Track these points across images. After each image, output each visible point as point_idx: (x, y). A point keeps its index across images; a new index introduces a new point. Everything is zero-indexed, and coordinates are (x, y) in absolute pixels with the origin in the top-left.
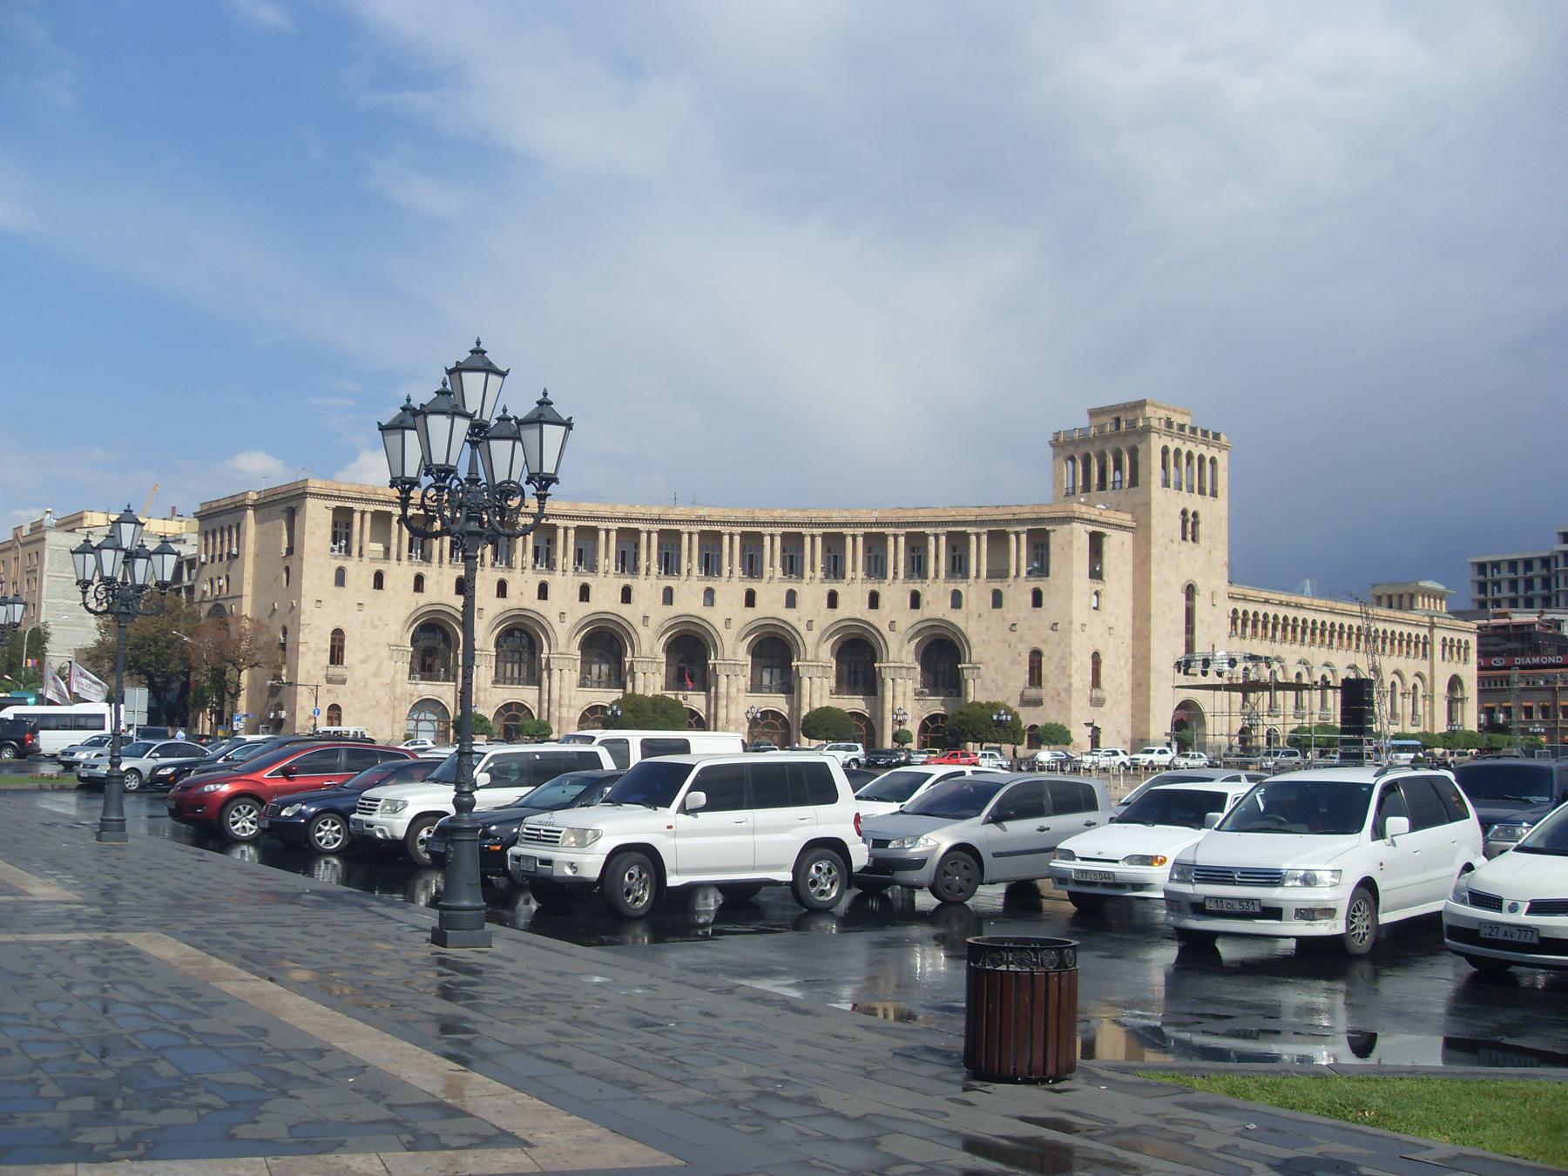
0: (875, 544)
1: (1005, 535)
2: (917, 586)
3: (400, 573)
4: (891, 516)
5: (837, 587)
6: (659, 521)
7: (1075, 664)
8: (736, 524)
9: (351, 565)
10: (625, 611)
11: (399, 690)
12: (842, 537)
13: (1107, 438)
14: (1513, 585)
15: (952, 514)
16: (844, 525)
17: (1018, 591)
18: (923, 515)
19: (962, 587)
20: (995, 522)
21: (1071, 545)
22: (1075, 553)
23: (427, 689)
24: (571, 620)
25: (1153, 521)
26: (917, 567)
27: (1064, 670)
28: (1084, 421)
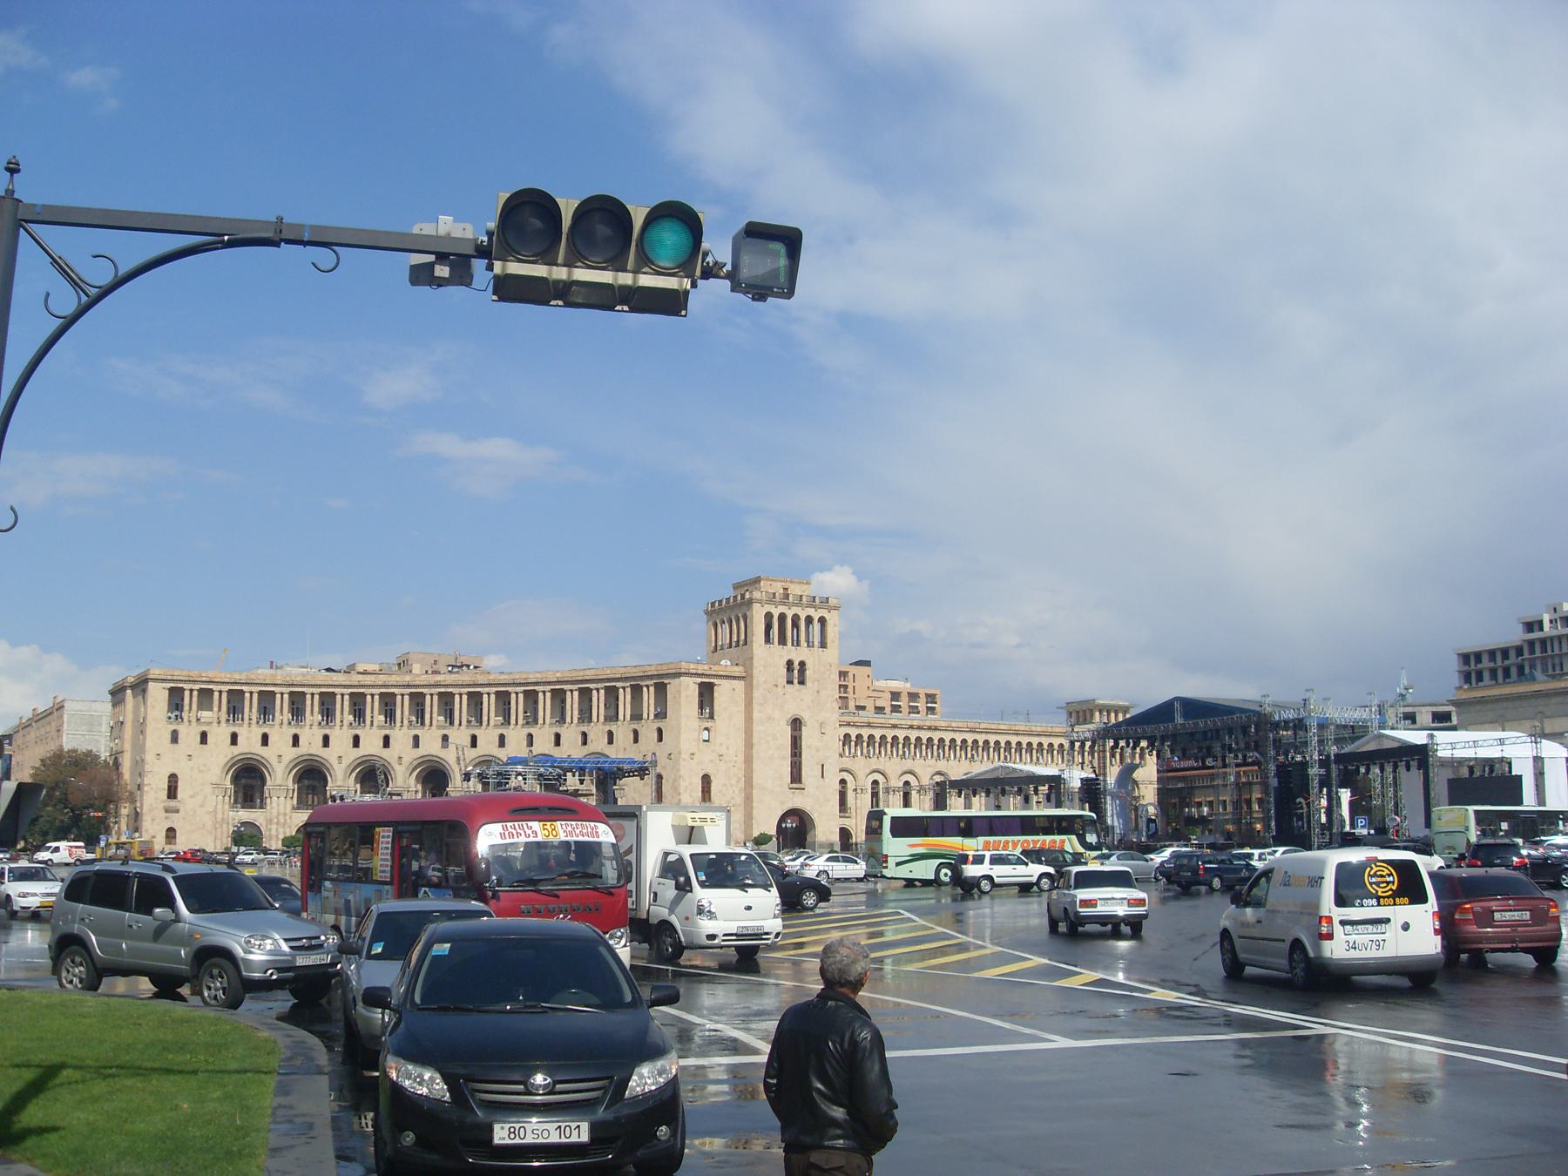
0: (559, 696)
2: (585, 729)
3: (219, 734)
4: (568, 676)
5: (532, 730)
6: (408, 686)
7: (683, 785)
8: (463, 686)
9: (183, 729)
10: (385, 753)
11: (220, 816)
13: (732, 608)
15: (609, 673)
17: (648, 731)
18: (590, 675)
20: (633, 678)
21: (685, 693)
22: (683, 700)
23: (245, 815)
24: (346, 762)
26: (586, 715)
27: (676, 789)
28: (730, 593)
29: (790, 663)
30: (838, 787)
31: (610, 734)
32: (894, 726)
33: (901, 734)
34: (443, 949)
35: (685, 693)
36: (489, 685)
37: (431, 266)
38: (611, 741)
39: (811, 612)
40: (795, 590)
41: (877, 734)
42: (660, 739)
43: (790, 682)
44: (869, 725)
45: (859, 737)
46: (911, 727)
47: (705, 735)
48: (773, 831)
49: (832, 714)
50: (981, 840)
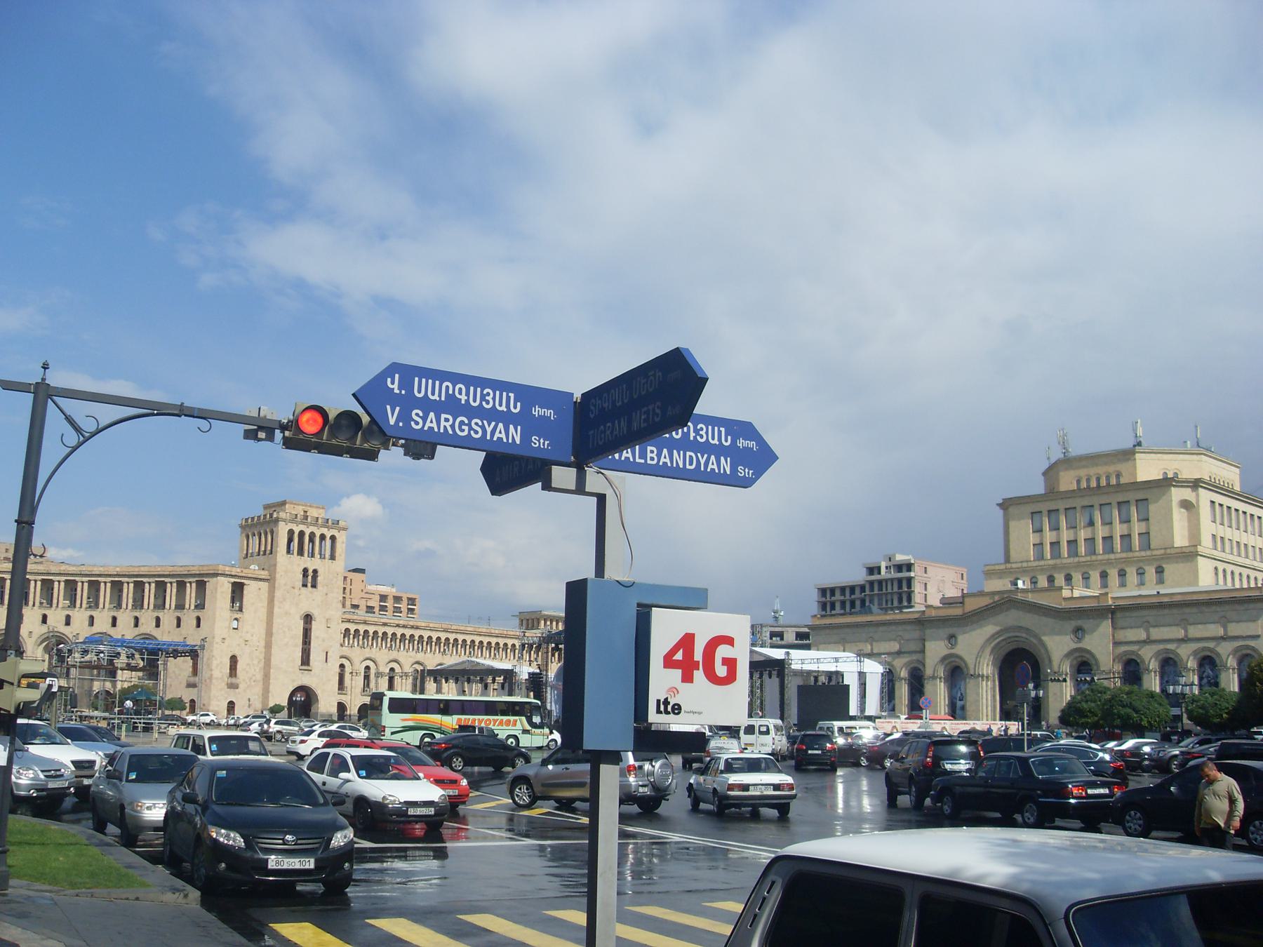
0: (117, 587)
1: (185, 583)
2: (137, 614)
4: (125, 571)
5: (94, 613)
7: (215, 663)
12: (98, 583)
13: (262, 524)
14: (843, 603)
15: (159, 571)
16: (100, 575)
17: (189, 618)
18: (144, 571)
19: (161, 615)
21: (220, 590)
22: (219, 595)
25: (278, 576)
26: (138, 603)
28: (261, 512)
29: (305, 571)
30: (338, 670)
31: (158, 619)
32: (385, 624)
33: (390, 631)
34: (223, 773)
35: (220, 590)
36: (60, 574)
37: (256, 432)
38: (158, 625)
39: (324, 531)
40: (313, 513)
41: (371, 629)
42: (198, 625)
43: (305, 585)
44: (365, 623)
45: (357, 631)
46: (398, 626)
47: (235, 624)
48: (285, 703)
49: (336, 612)
50: (456, 717)
